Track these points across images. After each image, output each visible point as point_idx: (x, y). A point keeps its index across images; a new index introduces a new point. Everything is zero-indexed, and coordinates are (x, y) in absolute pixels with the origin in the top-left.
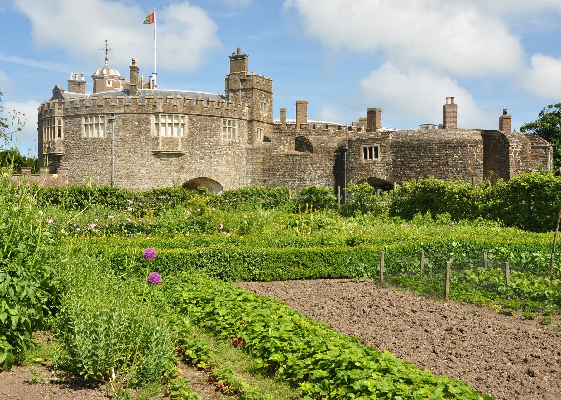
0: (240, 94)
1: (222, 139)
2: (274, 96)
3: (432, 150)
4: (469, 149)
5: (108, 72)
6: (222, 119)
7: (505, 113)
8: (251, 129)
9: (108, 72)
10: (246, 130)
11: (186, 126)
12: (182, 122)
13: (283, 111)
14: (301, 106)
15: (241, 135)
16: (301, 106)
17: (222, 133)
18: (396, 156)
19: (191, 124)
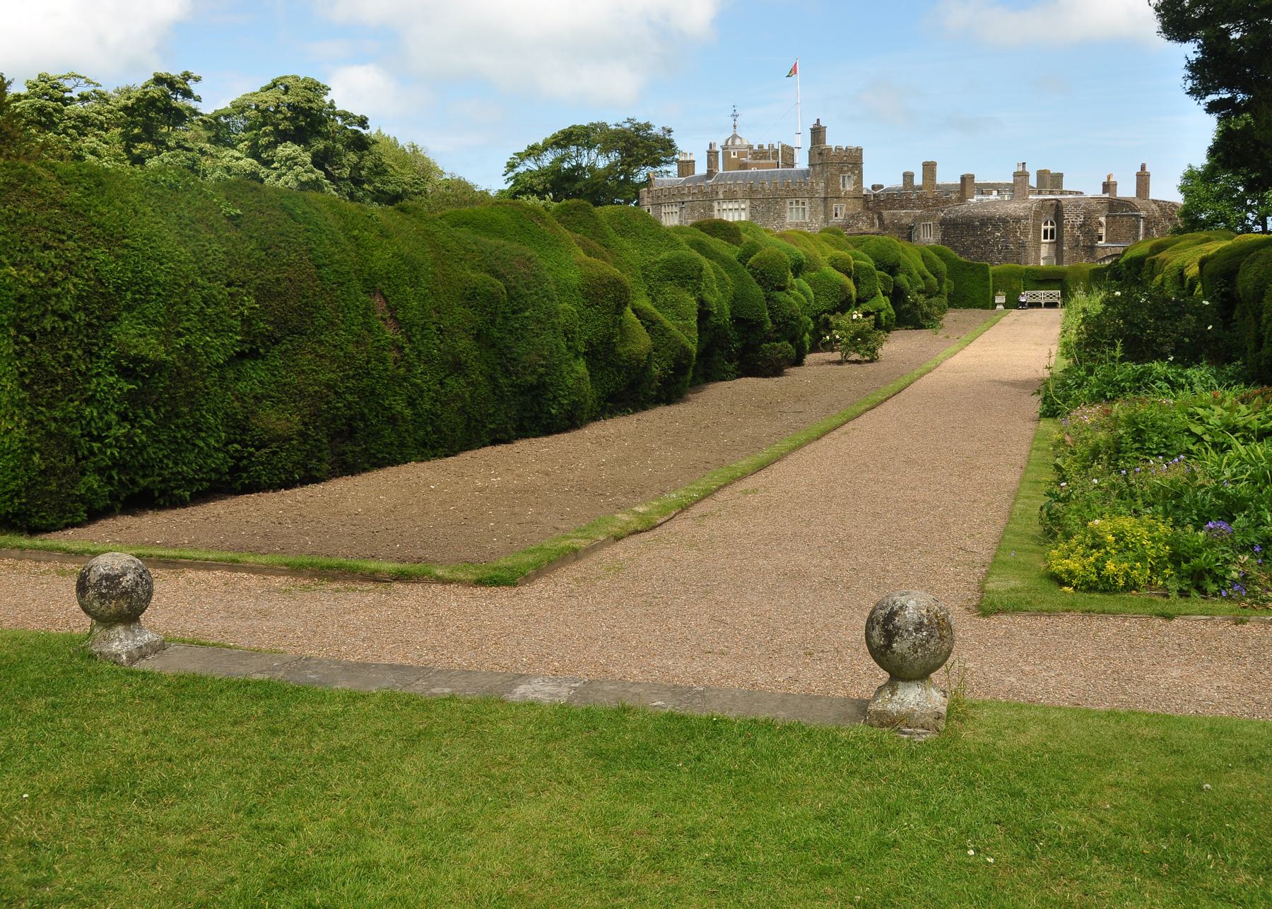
0: (818, 168)
1: (788, 220)
2: (864, 166)
3: (974, 228)
4: (1012, 225)
5: (733, 143)
6: (788, 201)
7: (1143, 167)
8: (826, 207)
9: (733, 143)
10: (821, 208)
11: (748, 210)
12: (743, 206)
13: (908, 177)
14: (929, 168)
15: (814, 213)
16: (929, 168)
17: (788, 215)
18: (944, 235)
19: (753, 208)
